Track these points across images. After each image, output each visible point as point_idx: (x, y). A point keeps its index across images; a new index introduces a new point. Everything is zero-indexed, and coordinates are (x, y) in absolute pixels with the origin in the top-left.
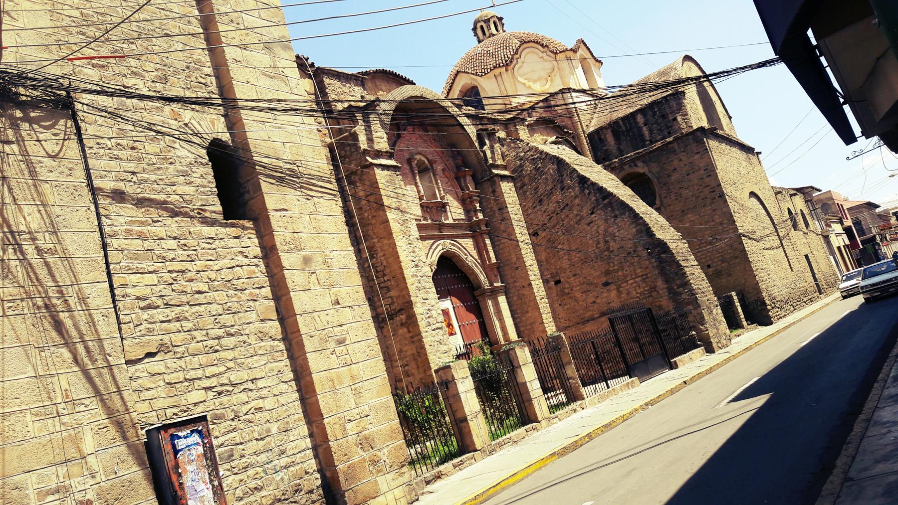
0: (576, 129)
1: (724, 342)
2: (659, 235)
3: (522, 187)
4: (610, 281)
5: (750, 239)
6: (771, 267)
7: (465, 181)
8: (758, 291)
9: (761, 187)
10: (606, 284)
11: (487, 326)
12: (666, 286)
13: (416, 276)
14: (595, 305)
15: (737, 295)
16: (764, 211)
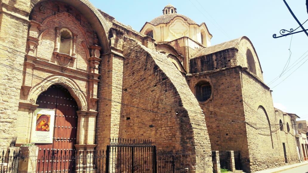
0: (185, 55)
2: (186, 106)
3: (127, 64)
4: (153, 125)
5: (251, 126)
6: (260, 144)
7: (94, 51)
8: (247, 154)
9: (268, 106)
10: (151, 126)
11: (77, 132)
12: (181, 136)
13: (5, 85)
14: (142, 136)
15: (234, 153)
16: (266, 117)
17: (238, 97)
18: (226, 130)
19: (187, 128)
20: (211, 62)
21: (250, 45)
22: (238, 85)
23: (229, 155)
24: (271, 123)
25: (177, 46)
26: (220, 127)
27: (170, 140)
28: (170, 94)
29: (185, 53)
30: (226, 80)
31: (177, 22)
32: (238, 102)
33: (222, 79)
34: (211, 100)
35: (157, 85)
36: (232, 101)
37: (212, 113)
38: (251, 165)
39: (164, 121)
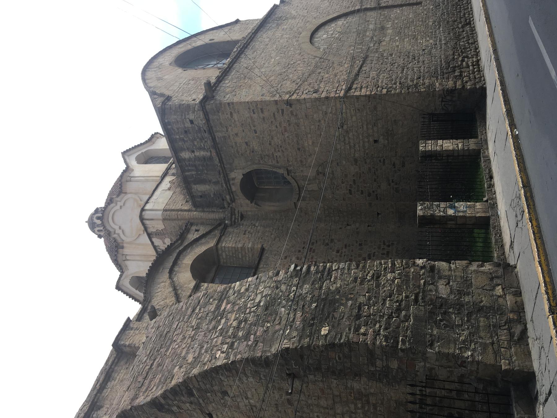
1: (510, 300)
5: (357, 75)
12: (364, 379)
16: (340, 22)
17: (280, 111)
18: (364, 142)
19: (340, 358)
20: (197, 163)
21: (168, 53)
22: (249, 108)
23: (430, 156)
24: (357, 8)
25: (164, 234)
26: (357, 155)
27: (375, 408)
28: (233, 386)
29: (178, 219)
30: (237, 134)
31: (113, 222)
32: (292, 113)
33: (236, 143)
34: (289, 172)
35: (208, 413)
36: (289, 125)
37: (321, 173)
38: (464, 86)
39: (316, 414)
